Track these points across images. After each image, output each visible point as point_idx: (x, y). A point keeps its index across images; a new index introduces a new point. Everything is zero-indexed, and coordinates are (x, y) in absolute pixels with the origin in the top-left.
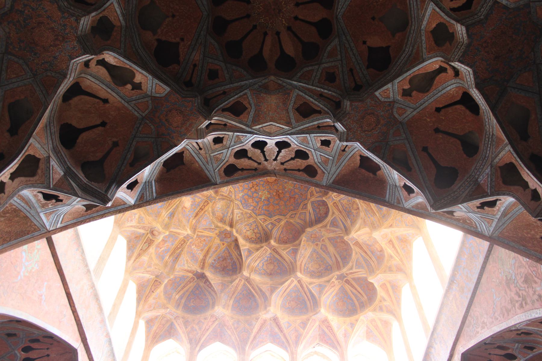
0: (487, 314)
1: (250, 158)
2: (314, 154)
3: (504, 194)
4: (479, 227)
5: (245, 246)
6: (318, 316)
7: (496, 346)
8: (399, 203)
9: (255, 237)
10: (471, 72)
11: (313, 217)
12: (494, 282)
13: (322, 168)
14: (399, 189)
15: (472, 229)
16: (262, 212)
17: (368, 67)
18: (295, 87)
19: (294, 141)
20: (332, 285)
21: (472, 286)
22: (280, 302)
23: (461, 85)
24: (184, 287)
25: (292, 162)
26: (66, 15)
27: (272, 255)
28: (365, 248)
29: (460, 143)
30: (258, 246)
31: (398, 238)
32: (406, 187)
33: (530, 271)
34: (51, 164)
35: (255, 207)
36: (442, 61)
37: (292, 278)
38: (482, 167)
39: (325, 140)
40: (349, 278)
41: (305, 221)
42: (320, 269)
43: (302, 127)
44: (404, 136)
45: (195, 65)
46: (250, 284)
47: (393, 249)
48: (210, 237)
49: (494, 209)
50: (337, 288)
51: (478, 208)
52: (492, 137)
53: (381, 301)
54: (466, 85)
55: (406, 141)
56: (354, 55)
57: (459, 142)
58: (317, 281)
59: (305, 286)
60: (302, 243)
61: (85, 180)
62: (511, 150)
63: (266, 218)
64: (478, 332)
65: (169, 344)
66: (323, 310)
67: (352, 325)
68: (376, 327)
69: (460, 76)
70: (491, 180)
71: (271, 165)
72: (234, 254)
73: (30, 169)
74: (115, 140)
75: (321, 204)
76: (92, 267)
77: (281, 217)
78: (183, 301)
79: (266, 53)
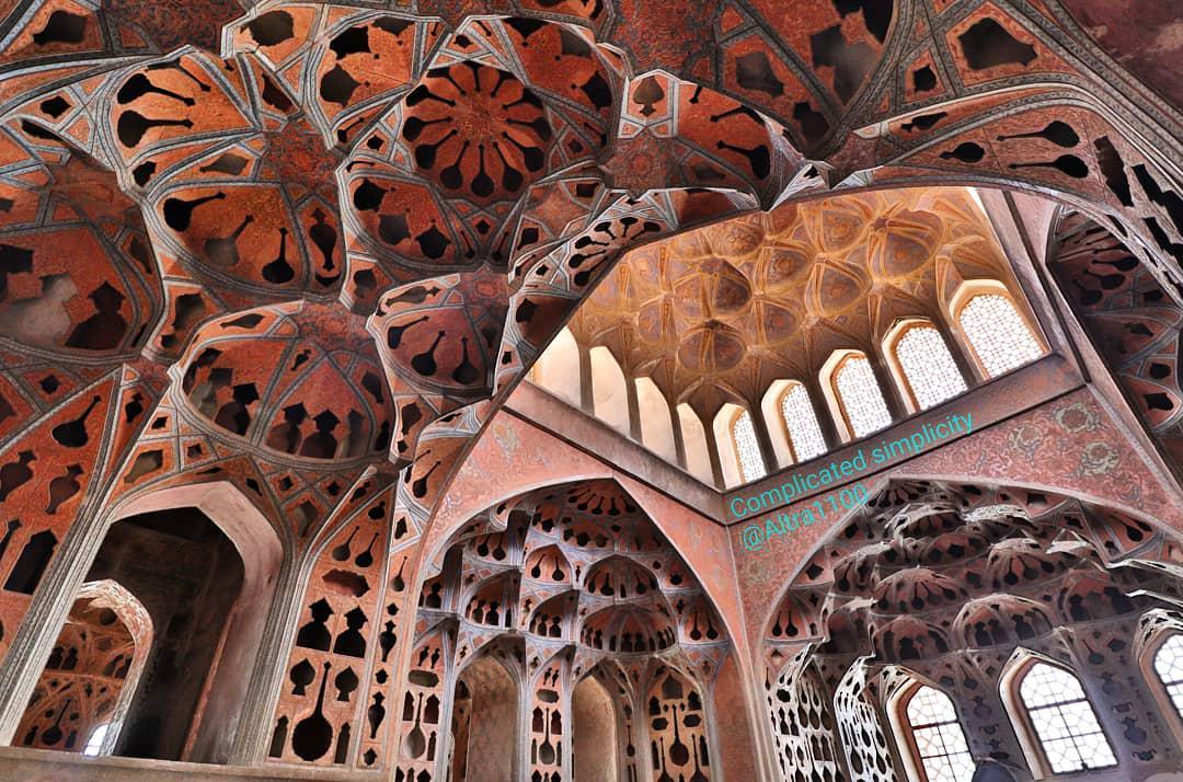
1: (589, 256)
5: (740, 261)
17: (598, 110)
18: (558, 179)
22: (817, 299)
24: (704, 347)
26: (329, 305)
30: (755, 252)
34: (425, 398)
40: (891, 217)
45: (463, 233)
46: (769, 300)
48: (697, 278)
50: (883, 238)
53: (949, 225)
56: (575, 108)
58: (850, 248)
59: (837, 263)
61: (463, 387)
65: (728, 410)
71: (613, 246)
72: (733, 277)
73: (413, 416)
74: (461, 338)
76: (576, 401)
78: (713, 359)
79: (512, 164)
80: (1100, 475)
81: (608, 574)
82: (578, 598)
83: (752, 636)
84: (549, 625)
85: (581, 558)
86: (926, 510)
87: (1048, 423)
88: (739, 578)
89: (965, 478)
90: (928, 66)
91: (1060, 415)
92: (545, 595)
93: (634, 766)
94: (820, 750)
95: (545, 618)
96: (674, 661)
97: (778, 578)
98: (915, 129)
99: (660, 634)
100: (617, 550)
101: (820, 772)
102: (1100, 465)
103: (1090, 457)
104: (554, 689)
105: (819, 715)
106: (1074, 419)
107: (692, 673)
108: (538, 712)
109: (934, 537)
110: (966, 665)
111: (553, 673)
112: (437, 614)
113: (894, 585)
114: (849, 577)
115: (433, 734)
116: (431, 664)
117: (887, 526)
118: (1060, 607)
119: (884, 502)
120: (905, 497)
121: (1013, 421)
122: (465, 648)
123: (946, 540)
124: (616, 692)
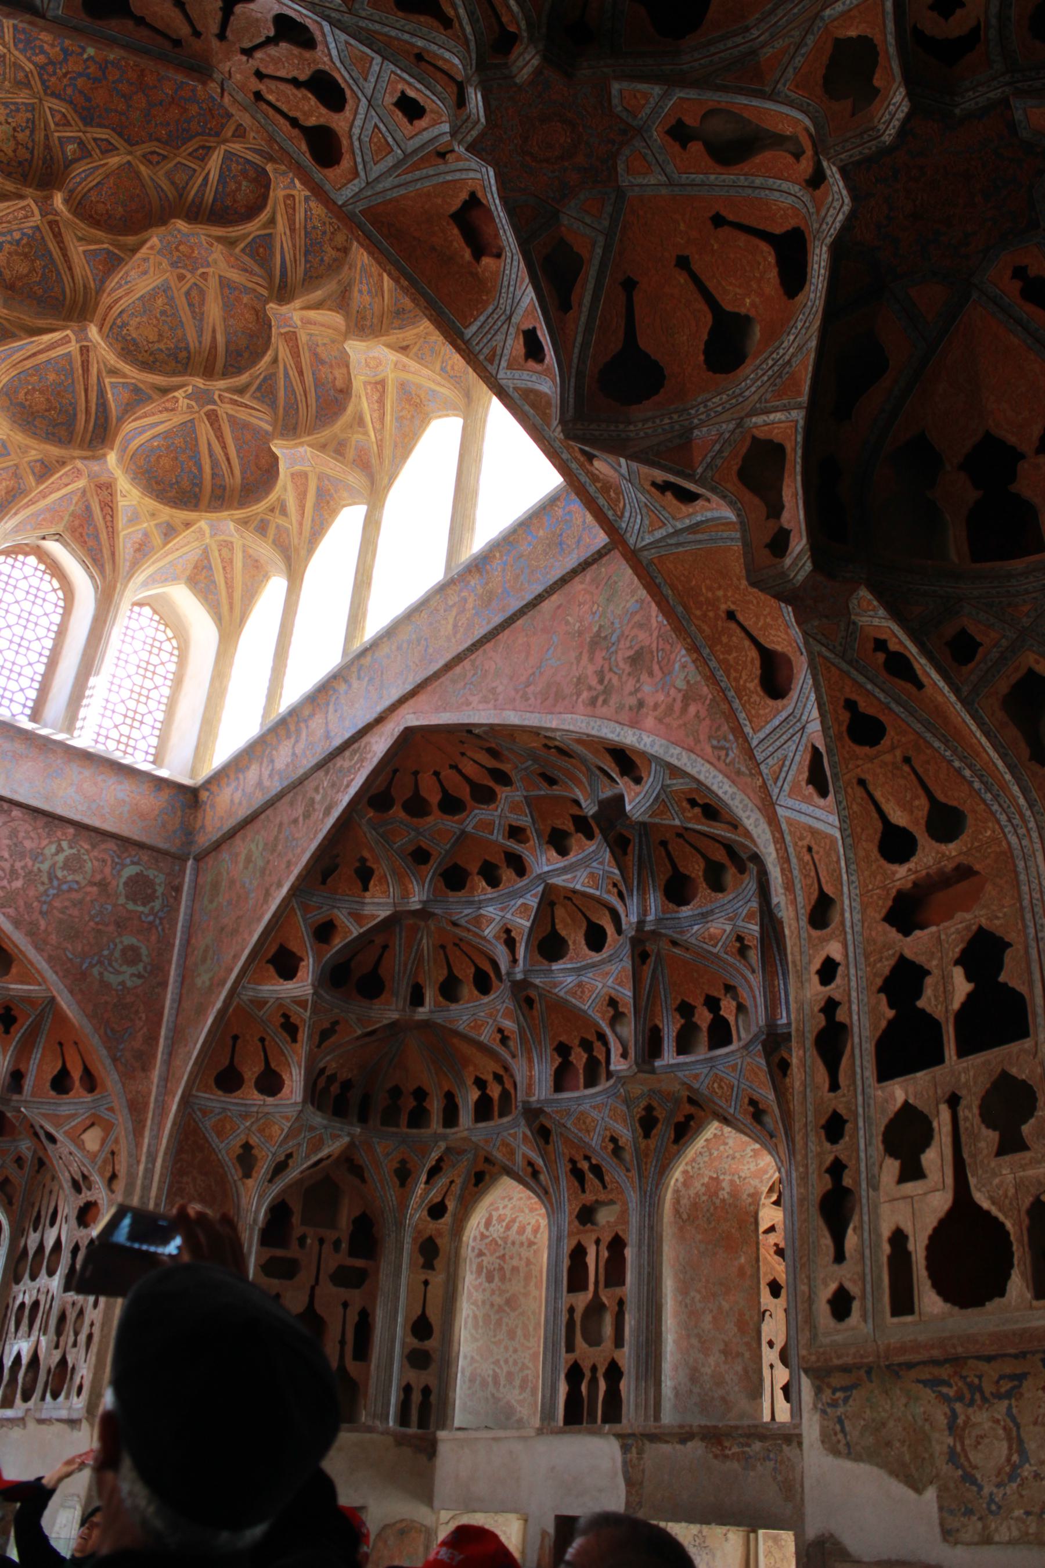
0: (511, 678)
2: (362, 110)
3: (724, 497)
4: (626, 519)
6: (95, 466)
7: (488, 745)
8: (491, 362)
9: (11, 154)
10: (846, 209)
11: (209, 196)
12: (567, 623)
13: (359, 160)
14: (512, 330)
15: (610, 513)
16: (69, 91)
19: (333, 49)
20: (169, 405)
21: (515, 604)
23: (804, 211)
25: (289, 89)
27: (38, 235)
28: (306, 358)
29: (710, 323)
31: (402, 386)
32: (531, 338)
33: (654, 646)
35: (51, 62)
36: (807, 129)
37: (68, 332)
38: (719, 409)
39: (414, 101)
40: (224, 410)
41: (181, 192)
42: (157, 346)
43: (377, 27)
44: (606, 223)
47: (376, 406)
49: (683, 508)
50: (177, 419)
51: (654, 484)
52: (784, 366)
53: (272, 510)
54: (816, 226)
55: (601, 240)
57: (708, 319)
59: (94, 371)
60: (144, 250)
62: (801, 423)
63: (71, 116)
64: (468, 703)
66: (112, 458)
67: (170, 532)
68: (228, 564)
69: (818, 193)
70: (720, 451)
75: (252, 174)
77: (116, 141)
87: (108, 870)
90: (981, 644)
91: (130, 871)
98: (881, 657)
102: (119, 973)
103: (117, 954)
106: (140, 888)
121: (71, 830)
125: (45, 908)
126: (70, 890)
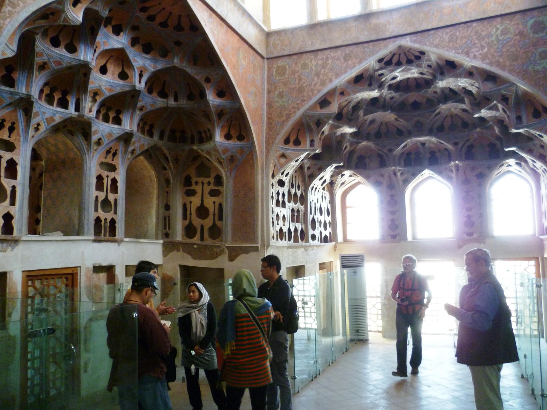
80: (538, 71)
81: (165, 81)
82: (139, 96)
83: (269, 142)
84: (112, 115)
85: (142, 63)
86: (413, 73)
87: (521, 27)
88: (268, 98)
89: (451, 55)
91: (531, 22)
92: (110, 90)
93: (169, 217)
94: (295, 216)
95: (109, 109)
96: (208, 153)
97: (298, 104)
99: (200, 133)
100: (176, 62)
101: (292, 229)
103: (537, 57)
104: (113, 163)
105: (299, 196)
107: (220, 163)
108: (100, 178)
109: (406, 93)
110: (393, 176)
111: (113, 151)
112: (11, 93)
113: (368, 122)
114: (345, 110)
115: (14, 187)
116: (8, 134)
117: (383, 79)
118: (461, 150)
119: (388, 62)
120: (404, 60)
122: (38, 124)
123: (412, 97)
124: (160, 169)
125: (500, 53)
126: (508, 42)
